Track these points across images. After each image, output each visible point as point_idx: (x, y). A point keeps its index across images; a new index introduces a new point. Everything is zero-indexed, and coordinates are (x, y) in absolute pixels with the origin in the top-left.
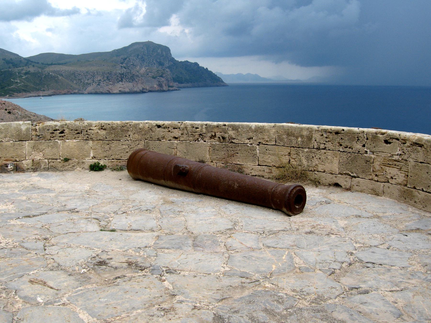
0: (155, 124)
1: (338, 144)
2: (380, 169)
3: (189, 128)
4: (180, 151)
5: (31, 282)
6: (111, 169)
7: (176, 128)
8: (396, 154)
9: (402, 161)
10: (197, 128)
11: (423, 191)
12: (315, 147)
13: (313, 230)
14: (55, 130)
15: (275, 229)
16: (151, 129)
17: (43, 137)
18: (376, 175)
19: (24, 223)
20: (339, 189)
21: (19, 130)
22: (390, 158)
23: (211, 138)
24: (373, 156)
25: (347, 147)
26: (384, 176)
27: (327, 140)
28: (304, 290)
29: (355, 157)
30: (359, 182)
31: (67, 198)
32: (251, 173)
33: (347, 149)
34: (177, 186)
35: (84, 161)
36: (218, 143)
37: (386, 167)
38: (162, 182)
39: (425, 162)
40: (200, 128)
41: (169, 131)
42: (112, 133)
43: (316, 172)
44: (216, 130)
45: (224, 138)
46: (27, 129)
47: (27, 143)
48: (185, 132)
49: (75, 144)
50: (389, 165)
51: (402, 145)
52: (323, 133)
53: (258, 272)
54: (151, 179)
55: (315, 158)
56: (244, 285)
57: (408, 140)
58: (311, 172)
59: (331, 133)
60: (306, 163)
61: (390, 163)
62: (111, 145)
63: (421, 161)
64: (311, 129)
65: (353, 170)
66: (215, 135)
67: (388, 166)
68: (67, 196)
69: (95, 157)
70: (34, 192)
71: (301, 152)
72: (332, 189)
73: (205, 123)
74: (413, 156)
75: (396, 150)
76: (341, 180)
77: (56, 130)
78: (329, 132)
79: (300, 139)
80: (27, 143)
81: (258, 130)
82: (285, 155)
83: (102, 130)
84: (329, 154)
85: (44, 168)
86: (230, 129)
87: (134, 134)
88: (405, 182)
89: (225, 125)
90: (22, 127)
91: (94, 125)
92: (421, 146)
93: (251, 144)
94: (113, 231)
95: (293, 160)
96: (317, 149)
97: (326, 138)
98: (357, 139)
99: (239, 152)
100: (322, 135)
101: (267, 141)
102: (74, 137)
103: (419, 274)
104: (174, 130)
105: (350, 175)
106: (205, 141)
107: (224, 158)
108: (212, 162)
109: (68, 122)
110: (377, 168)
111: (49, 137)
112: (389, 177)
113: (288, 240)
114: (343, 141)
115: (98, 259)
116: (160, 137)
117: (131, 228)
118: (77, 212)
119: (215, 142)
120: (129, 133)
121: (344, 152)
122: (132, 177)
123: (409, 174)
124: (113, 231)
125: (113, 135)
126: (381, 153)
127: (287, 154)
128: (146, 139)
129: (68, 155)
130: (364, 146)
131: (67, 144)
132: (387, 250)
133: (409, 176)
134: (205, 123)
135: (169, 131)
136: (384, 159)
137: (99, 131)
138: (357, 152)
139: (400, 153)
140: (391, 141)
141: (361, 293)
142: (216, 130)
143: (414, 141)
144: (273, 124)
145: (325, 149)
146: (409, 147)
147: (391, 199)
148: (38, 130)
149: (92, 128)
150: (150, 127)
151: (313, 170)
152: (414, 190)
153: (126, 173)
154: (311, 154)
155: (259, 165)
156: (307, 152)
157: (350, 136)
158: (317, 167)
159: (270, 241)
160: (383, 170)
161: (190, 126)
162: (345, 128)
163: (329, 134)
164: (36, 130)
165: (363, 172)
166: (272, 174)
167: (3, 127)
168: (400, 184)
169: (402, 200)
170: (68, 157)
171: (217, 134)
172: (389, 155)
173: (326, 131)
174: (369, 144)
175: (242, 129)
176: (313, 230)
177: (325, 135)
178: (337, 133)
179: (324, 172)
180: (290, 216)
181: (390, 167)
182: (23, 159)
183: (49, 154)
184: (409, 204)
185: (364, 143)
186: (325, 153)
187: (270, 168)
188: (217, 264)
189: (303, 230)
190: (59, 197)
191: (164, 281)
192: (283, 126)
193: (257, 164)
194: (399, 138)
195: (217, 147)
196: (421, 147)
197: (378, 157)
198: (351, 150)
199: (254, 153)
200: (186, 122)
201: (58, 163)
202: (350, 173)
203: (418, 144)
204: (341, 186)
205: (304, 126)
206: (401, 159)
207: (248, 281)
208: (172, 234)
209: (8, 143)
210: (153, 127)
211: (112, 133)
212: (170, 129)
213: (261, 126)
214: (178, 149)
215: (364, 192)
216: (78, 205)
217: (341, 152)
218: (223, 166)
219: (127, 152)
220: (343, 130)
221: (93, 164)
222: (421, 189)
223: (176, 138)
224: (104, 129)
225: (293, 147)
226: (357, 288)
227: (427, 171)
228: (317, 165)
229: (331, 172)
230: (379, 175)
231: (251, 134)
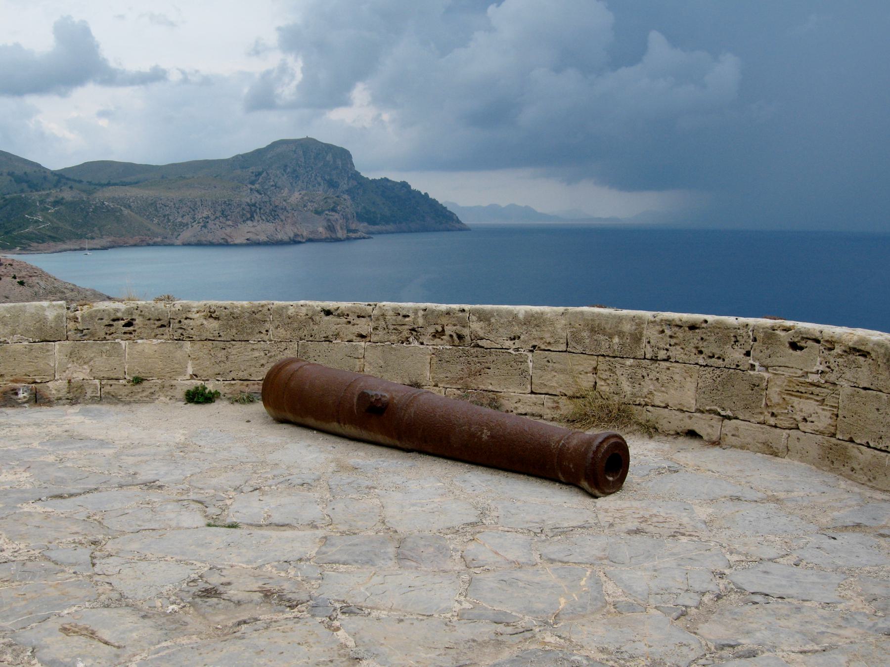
0: (319, 308)
1: (694, 351)
2: (781, 401)
3: (390, 316)
4: (370, 364)
5: (65, 630)
6: (229, 399)
7: (363, 317)
8: (814, 370)
9: (826, 385)
10: (405, 316)
11: (869, 447)
12: (648, 356)
13: (643, 525)
14: (114, 320)
15: (566, 525)
16: (311, 318)
17: (90, 333)
18: (773, 414)
19: (50, 510)
20: (695, 443)
21: (41, 320)
22: (802, 379)
23: (434, 336)
24: (766, 375)
25: (713, 357)
26: (790, 416)
27: (673, 341)
28: (623, 649)
29: (729, 376)
30: (737, 429)
31: (140, 459)
32: (516, 408)
33: (713, 359)
34: (365, 434)
35: (173, 382)
36: (448, 347)
37: (793, 398)
38: (334, 426)
39: (872, 387)
40: (412, 316)
41: (349, 322)
42: (231, 326)
43: (649, 408)
44: (444, 320)
45: (460, 337)
46: (58, 318)
47: (57, 347)
48: (382, 323)
49: (156, 348)
50: (799, 394)
51: (826, 352)
52: (664, 327)
53: (530, 611)
54: (311, 421)
55: (647, 378)
56: (500, 638)
58: (639, 407)
59: (680, 327)
60: (630, 388)
61: (801, 389)
62: (229, 350)
63: (866, 385)
64: (640, 318)
65: (726, 404)
66: (443, 330)
67: (796, 396)
68: (140, 455)
69: (196, 376)
70: (72, 446)
71: (618, 366)
72: (682, 442)
73: (423, 305)
75: (813, 361)
76: (700, 424)
77: (118, 320)
78: (677, 326)
79: (616, 340)
80: (57, 347)
81: (531, 321)
82: (587, 373)
83: (211, 320)
84: (677, 370)
85: (92, 398)
86: (474, 318)
87: (277, 328)
88: (832, 430)
89: (463, 311)
90: (47, 313)
91: (195, 310)
92: (865, 354)
93: (517, 350)
94: (233, 526)
95: (603, 383)
96: (652, 359)
97: (671, 337)
98: (733, 339)
99: (492, 366)
100: (663, 332)
101: (549, 343)
102: (153, 334)
103: (860, 618)
104: (358, 321)
105: (719, 414)
106: (422, 344)
107: (461, 379)
108: (436, 385)
109: (141, 303)
111: (102, 335)
112: (799, 418)
113: (591, 546)
114: (705, 343)
115: (201, 585)
116: (330, 334)
117: (271, 520)
118: (160, 487)
119: (443, 345)
120: (267, 326)
121: (707, 365)
122: (272, 416)
123: (840, 412)
124: (233, 526)
125: (234, 331)
127: (590, 369)
128: (301, 339)
129: (140, 370)
130: (748, 354)
131: (139, 348)
132: (795, 569)
133: (840, 417)
134: (423, 305)
135: (349, 322)
136: (790, 381)
137: (205, 322)
138: (734, 367)
139: (821, 368)
140: (803, 344)
141: (740, 657)
142: (444, 320)
143: (850, 344)
144: (561, 309)
145: (667, 359)
147: (803, 464)
148: (80, 320)
149: (190, 316)
150: (310, 314)
151: (643, 403)
152: (850, 445)
153: (259, 407)
154: (639, 371)
155: (532, 393)
156: (631, 366)
157: (720, 334)
158: (650, 396)
159: (554, 549)
160: (787, 404)
161: (391, 313)
162: (710, 318)
163: (676, 329)
164: (75, 319)
165: (746, 407)
167: (9, 312)
168: (822, 433)
169: (826, 466)
170: (141, 376)
171: (446, 328)
172: (800, 373)
173: (670, 323)
174: (758, 351)
175: (497, 318)
176: (643, 525)
177: (668, 332)
178: (693, 327)
179: (666, 407)
180: (596, 497)
181: (800, 397)
182: (48, 379)
183: (102, 369)
184: (841, 474)
185: (748, 348)
186: (668, 369)
187: (556, 398)
188: (445, 595)
189: (623, 526)
190: (122, 457)
191: (338, 629)
192: (582, 313)
193: (529, 390)
194: (820, 338)
195: (446, 356)
196: (865, 356)
197: (776, 377)
198: (721, 361)
199: (522, 367)
200: (384, 303)
201: (121, 388)
202: (719, 410)
203: (859, 351)
204: (701, 437)
205: (625, 312)
206: (823, 382)
207: (509, 630)
208: (354, 534)
209: (19, 347)
210: (315, 313)
211: (231, 326)
212: (350, 318)
213: (537, 313)
214: (368, 359)
215: (748, 449)
216: (162, 473)
217: (701, 366)
218: (459, 395)
219: (262, 365)
220: (706, 321)
221: (192, 388)
222: (864, 442)
223: (362, 336)
224: (215, 318)
225: (603, 355)
226: (733, 646)
227: (877, 406)
228: (651, 393)
229: (679, 407)
231: (516, 330)
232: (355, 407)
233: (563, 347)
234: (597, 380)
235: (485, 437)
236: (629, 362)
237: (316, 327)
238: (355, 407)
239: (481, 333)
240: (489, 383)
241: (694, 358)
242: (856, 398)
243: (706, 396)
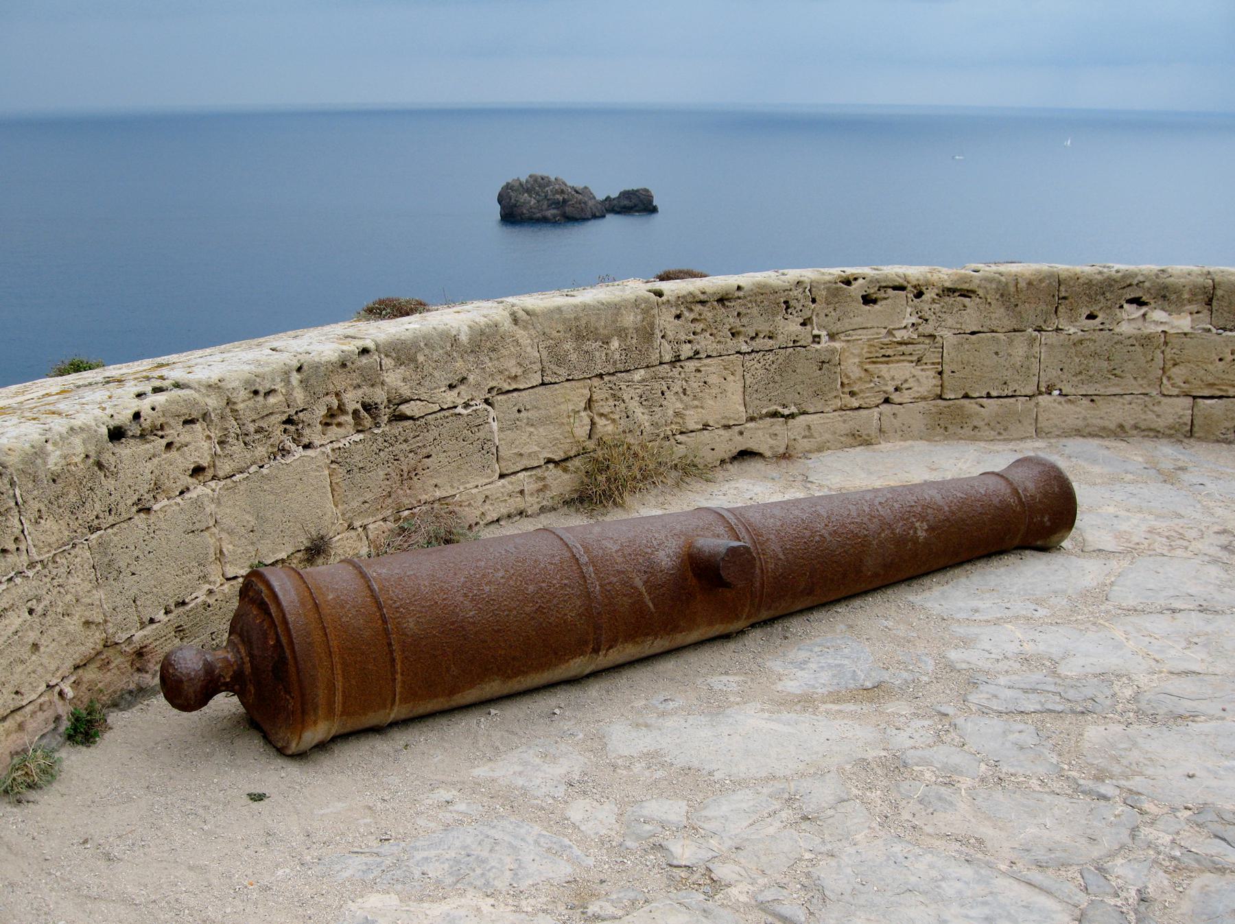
2: (863, 374)
4: (231, 532)
11: (989, 396)
18: (852, 394)
24: (837, 345)
27: (699, 327)
38: (577, 665)
39: (985, 329)
44: (339, 381)
45: (366, 407)
54: (494, 687)
57: (929, 284)
59: (703, 302)
60: (646, 417)
63: (975, 329)
74: (950, 321)
76: (759, 437)
79: (615, 344)
84: (712, 369)
88: (938, 390)
92: (966, 294)
93: (466, 405)
97: (693, 321)
110: (856, 372)
126: (860, 332)
128: (93, 530)
139: (914, 320)
143: (948, 285)
152: (966, 402)
154: (656, 385)
155: (502, 476)
156: (644, 380)
161: (243, 394)
163: (699, 307)
166: (548, 494)
168: (924, 399)
175: (427, 351)
178: (722, 300)
179: (706, 427)
181: (887, 363)
187: (539, 472)
193: (497, 475)
194: (905, 284)
195: (357, 458)
197: (851, 344)
198: (770, 343)
199: (481, 434)
202: (780, 409)
204: (760, 455)
218: (391, 531)
219: (35, 646)
220: (739, 288)
223: (198, 471)
225: (601, 376)
227: (995, 349)
228: (677, 414)
230: (862, 391)
232: (647, 598)
234: (597, 419)
235: (922, 534)
236: (638, 375)
237: (110, 484)
238: (647, 598)
239: (406, 391)
240: (427, 490)
241: (732, 344)
242: (966, 347)
243: (759, 396)
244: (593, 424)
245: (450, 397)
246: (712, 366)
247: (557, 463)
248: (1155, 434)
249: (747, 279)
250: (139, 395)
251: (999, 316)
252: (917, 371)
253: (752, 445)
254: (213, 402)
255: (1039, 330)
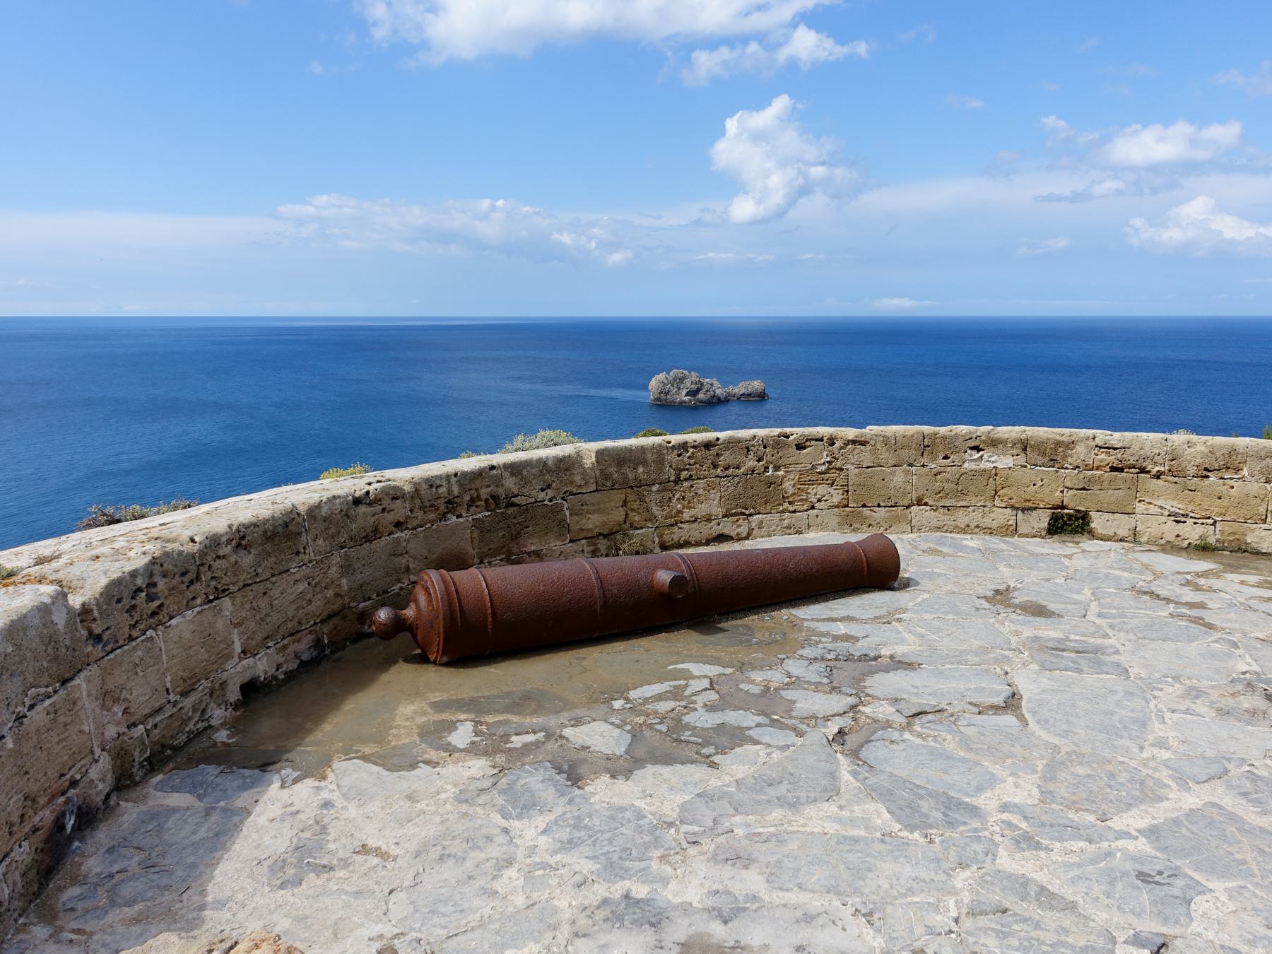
4: (414, 558)
11: (879, 506)
18: (790, 503)
35: (225, 676)
45: (495, 497)
48: (417, 502)
61: (812, 477)
71: (646, 493)
78: (694, 447)
79: (641, 469)
92: (863, 443)
93: (550, 500)
146: (842, 448)
148: (96, 614)
155: (571, 541)
161: (424, 486)
162: (723, 435)
168: (837, 507)
178: (708, 445)
212: (385, 503)
220: (718, 439)
225: (632, 487)
233: (593, 488)
236: (655, 488)
239: (515, 490)
244: (627, 515)
245: (542, 495)
246: (701, 484)
247: (605, 536)
248: (990, 531)
249: (723, 435)
250: (370, 484)
251: (885, 456)
252: (831, 490)
253: (726, 531)
254: (407, 488)
255: (911, 465)
